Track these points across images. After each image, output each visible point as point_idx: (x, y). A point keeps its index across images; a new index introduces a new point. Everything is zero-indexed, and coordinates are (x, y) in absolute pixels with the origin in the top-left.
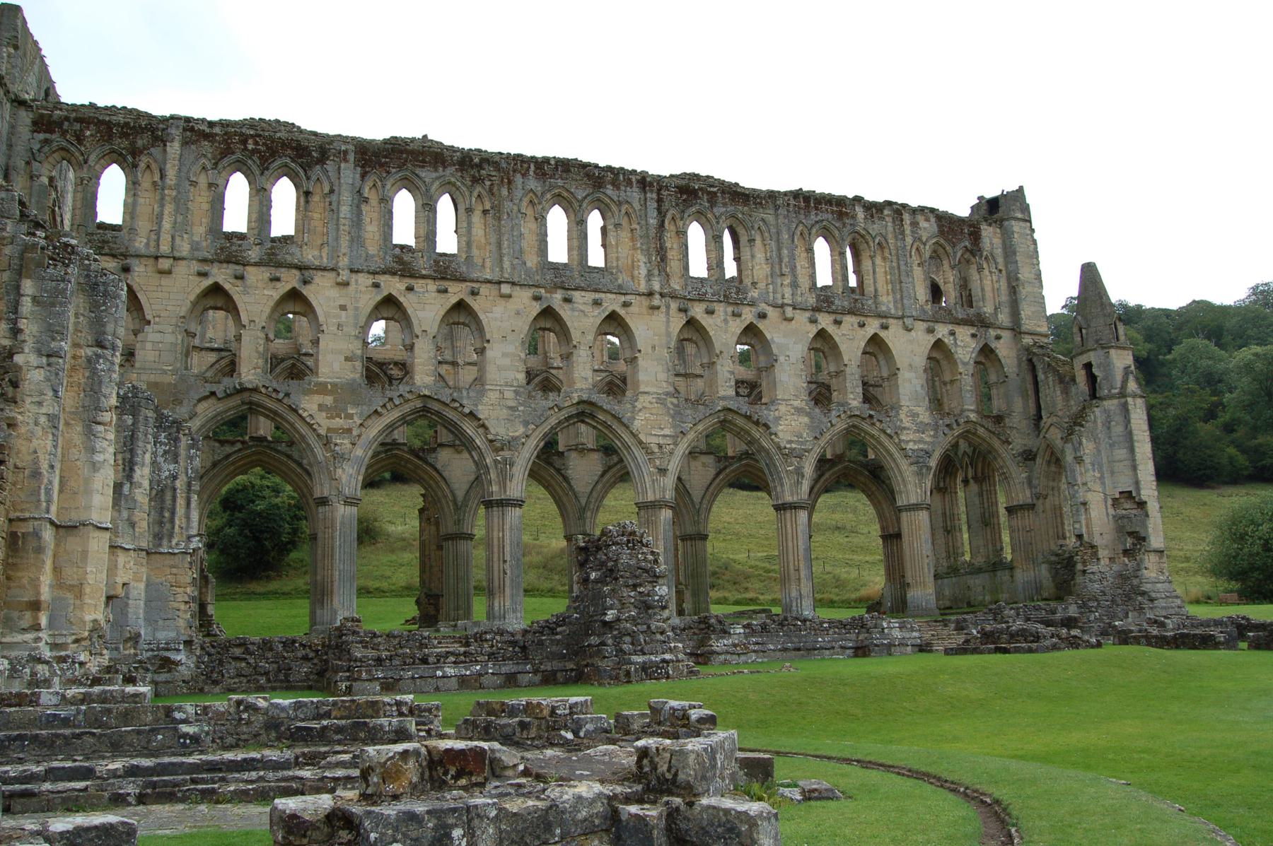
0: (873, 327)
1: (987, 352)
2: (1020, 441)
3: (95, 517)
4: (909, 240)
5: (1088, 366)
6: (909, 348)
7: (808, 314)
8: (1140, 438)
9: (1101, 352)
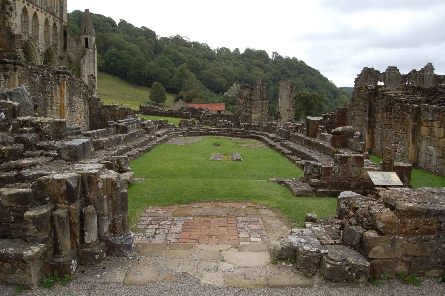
1: (55, 24)
2: (59, 54)
5: (86, 39)
6: (42, 17)
7: (28, 3)
9: (90, 36)
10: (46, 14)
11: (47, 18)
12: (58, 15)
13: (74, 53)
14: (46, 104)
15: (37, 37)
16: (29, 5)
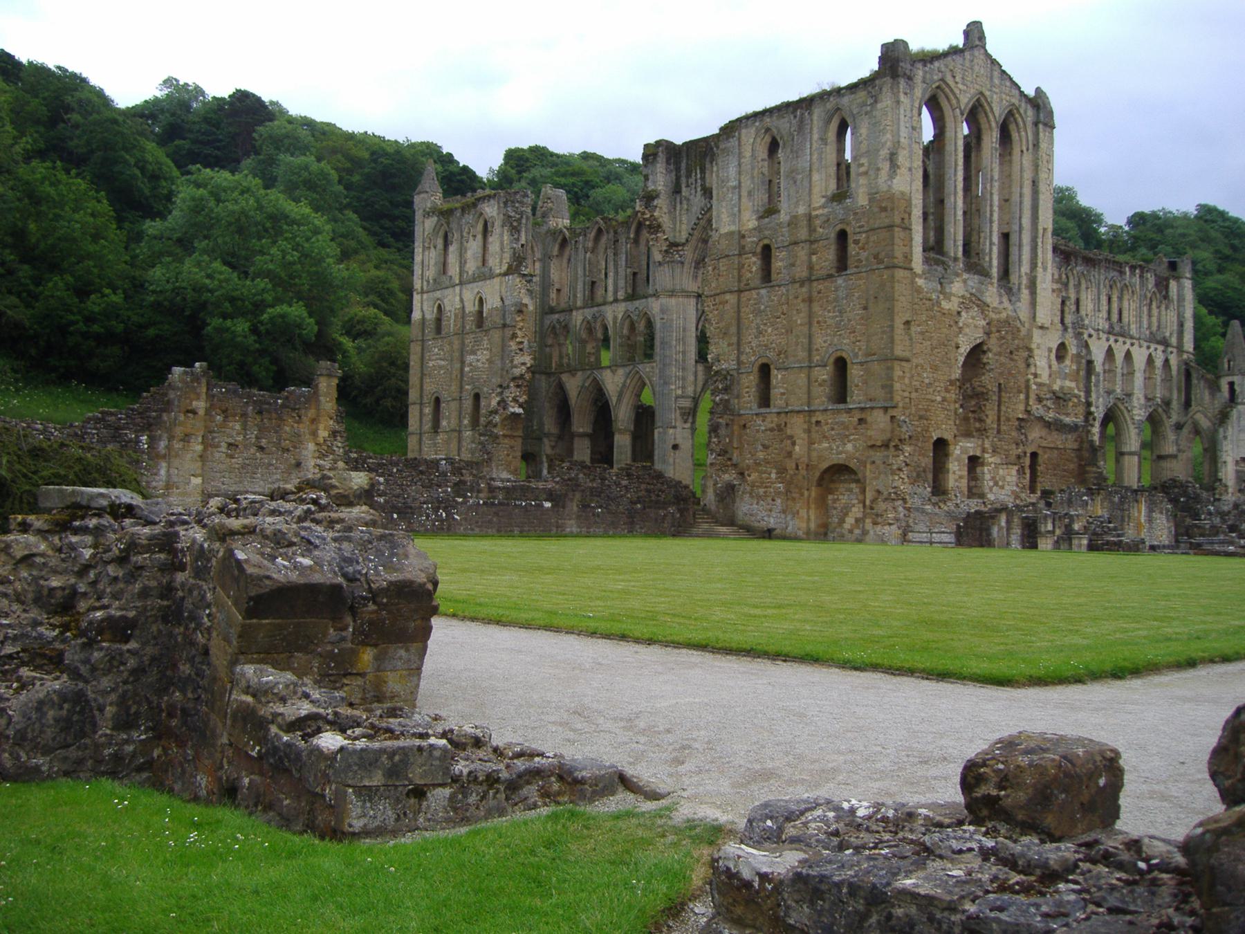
1: (1167, 361)
2: (1175, 418)
6: (1140, 356)
10: (1148, 348)
11: (1150, 355)
12: (1174, 341)
13: (1206, 416)
14: (1123, 520)
15: (1129, 395)
16: (1116, 341)
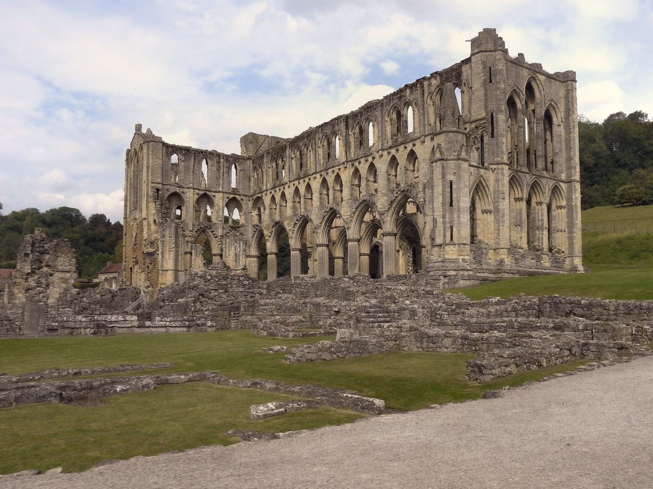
0: (410, 146)
3: (169, 268)
4: (426, 95)
8: (437, 184)
